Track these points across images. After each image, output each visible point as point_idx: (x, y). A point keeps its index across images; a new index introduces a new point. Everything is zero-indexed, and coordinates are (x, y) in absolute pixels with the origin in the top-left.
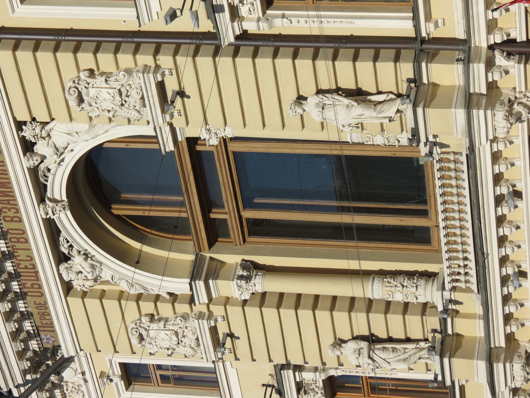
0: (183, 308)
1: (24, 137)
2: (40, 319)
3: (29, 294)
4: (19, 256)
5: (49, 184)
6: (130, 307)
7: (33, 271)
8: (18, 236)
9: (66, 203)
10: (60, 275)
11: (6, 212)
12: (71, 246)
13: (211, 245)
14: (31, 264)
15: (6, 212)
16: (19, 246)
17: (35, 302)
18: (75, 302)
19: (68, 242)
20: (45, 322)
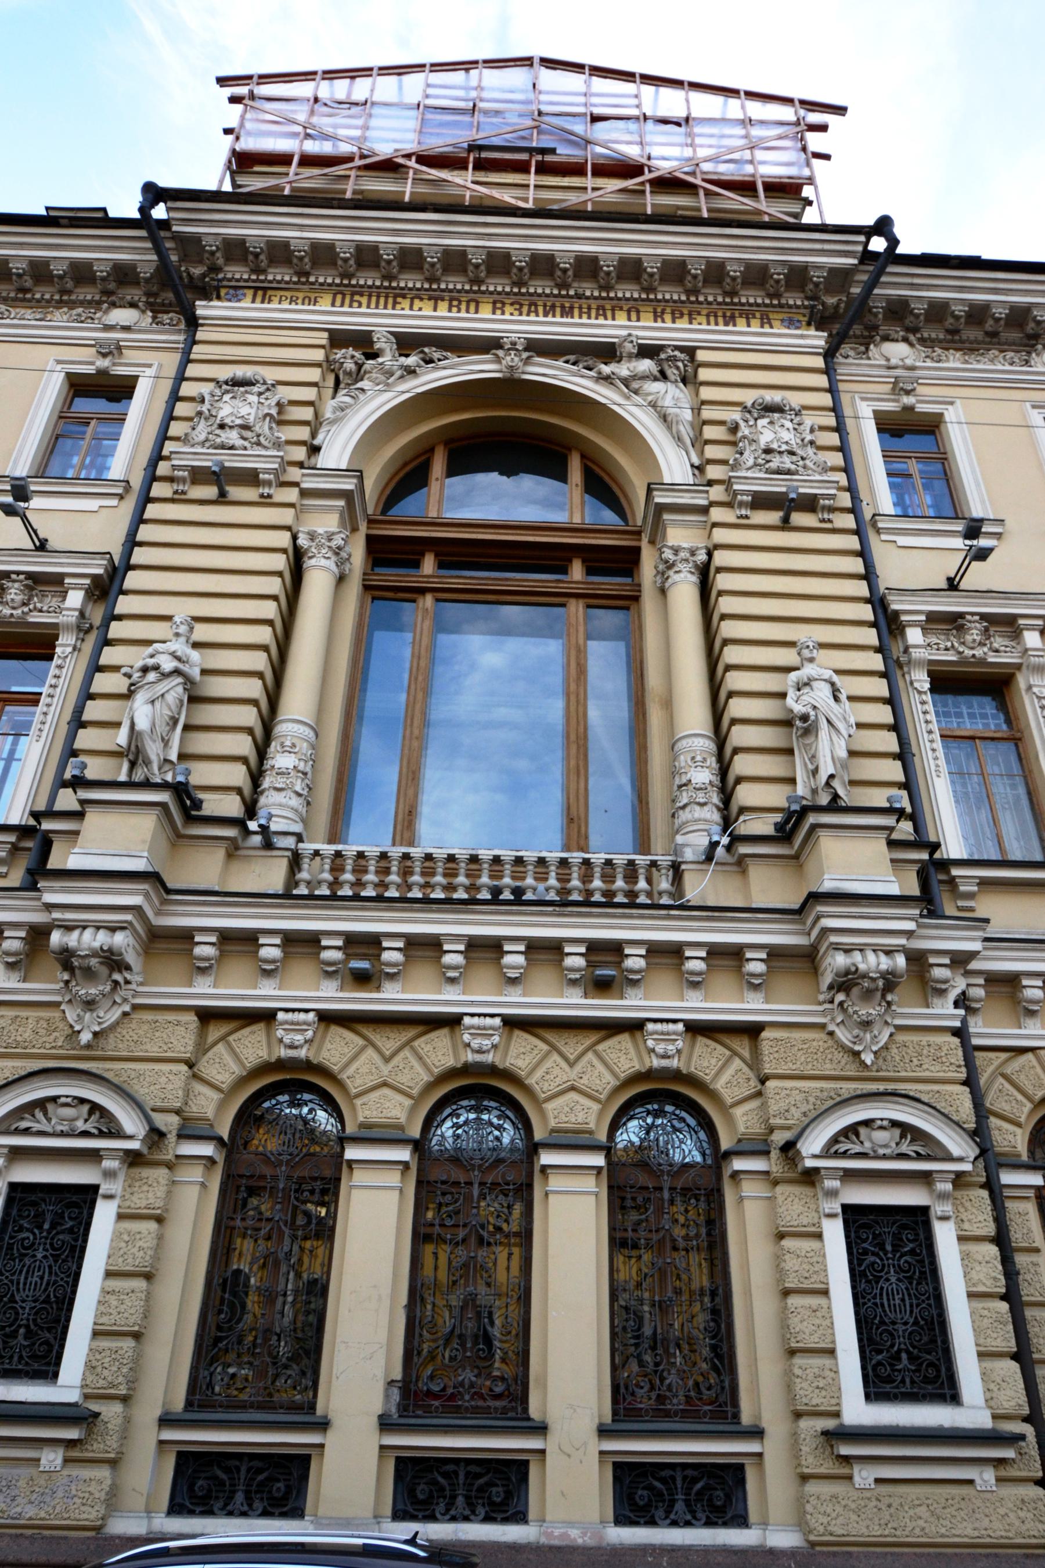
0: (300, 453)
5: (560, 363)
9: (516, 376)
12: (431, 361)
13: (370, 540)
18: (323, 338)
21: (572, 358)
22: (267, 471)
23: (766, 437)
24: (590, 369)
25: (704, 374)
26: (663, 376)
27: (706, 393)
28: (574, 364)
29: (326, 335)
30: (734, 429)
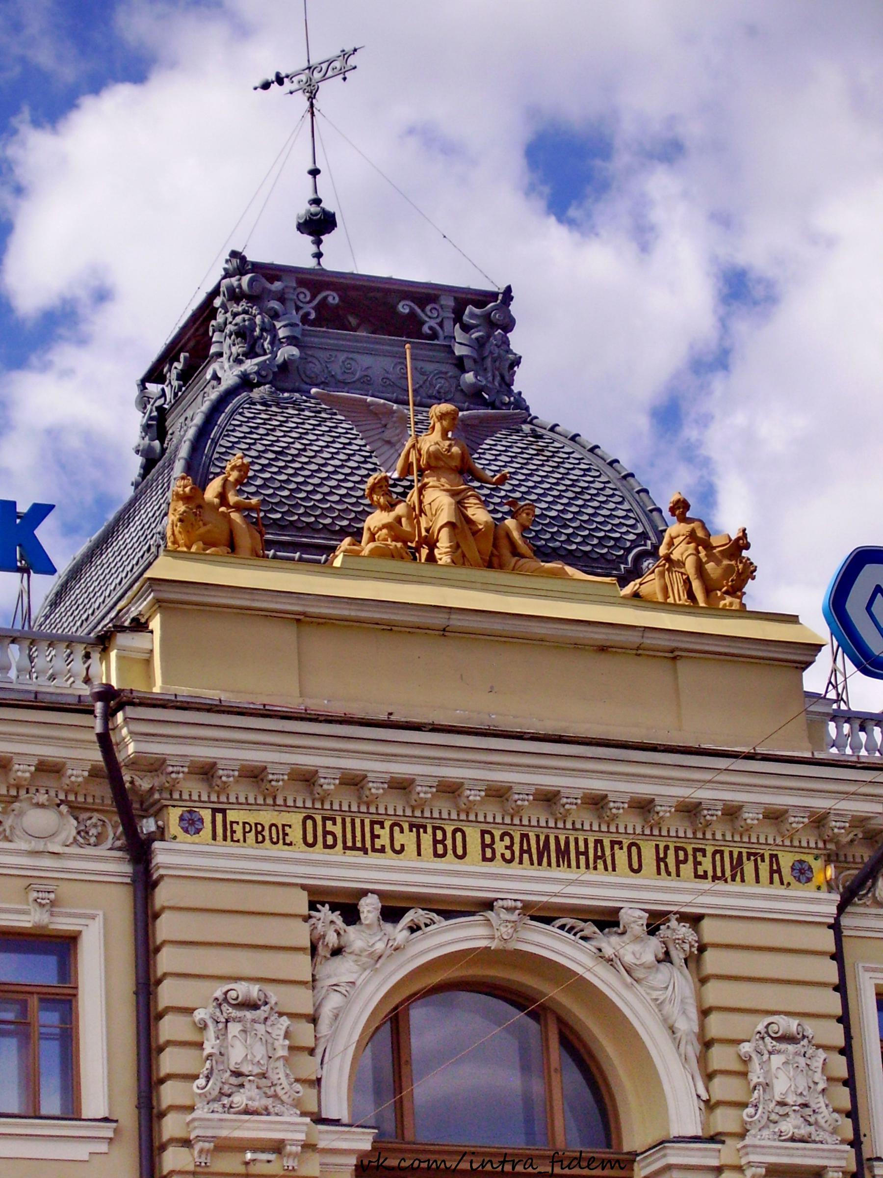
1: (669, 920)
2: (244, 823)
3: (309, 823)
4: (402, 831)
5: (552, 929)
6: (302, 1000)
7: (368, 844)
8: (449, 842)
10: (364, 893)
11: (502, 839)
14: (383, 846)
15: (502, 839)
16: (427, 839)
17: (290, 826)
19: (427, 925)
20: (238, 828)
21: (569, 921)
22: (294, 1142)
23: (781, 1086)
24: (585, 938)
25: (712, 961)
26: (667, 958)
27: (715, 993)
28: (569, 931)
29: (304, 895)
30: (746, 1061)
